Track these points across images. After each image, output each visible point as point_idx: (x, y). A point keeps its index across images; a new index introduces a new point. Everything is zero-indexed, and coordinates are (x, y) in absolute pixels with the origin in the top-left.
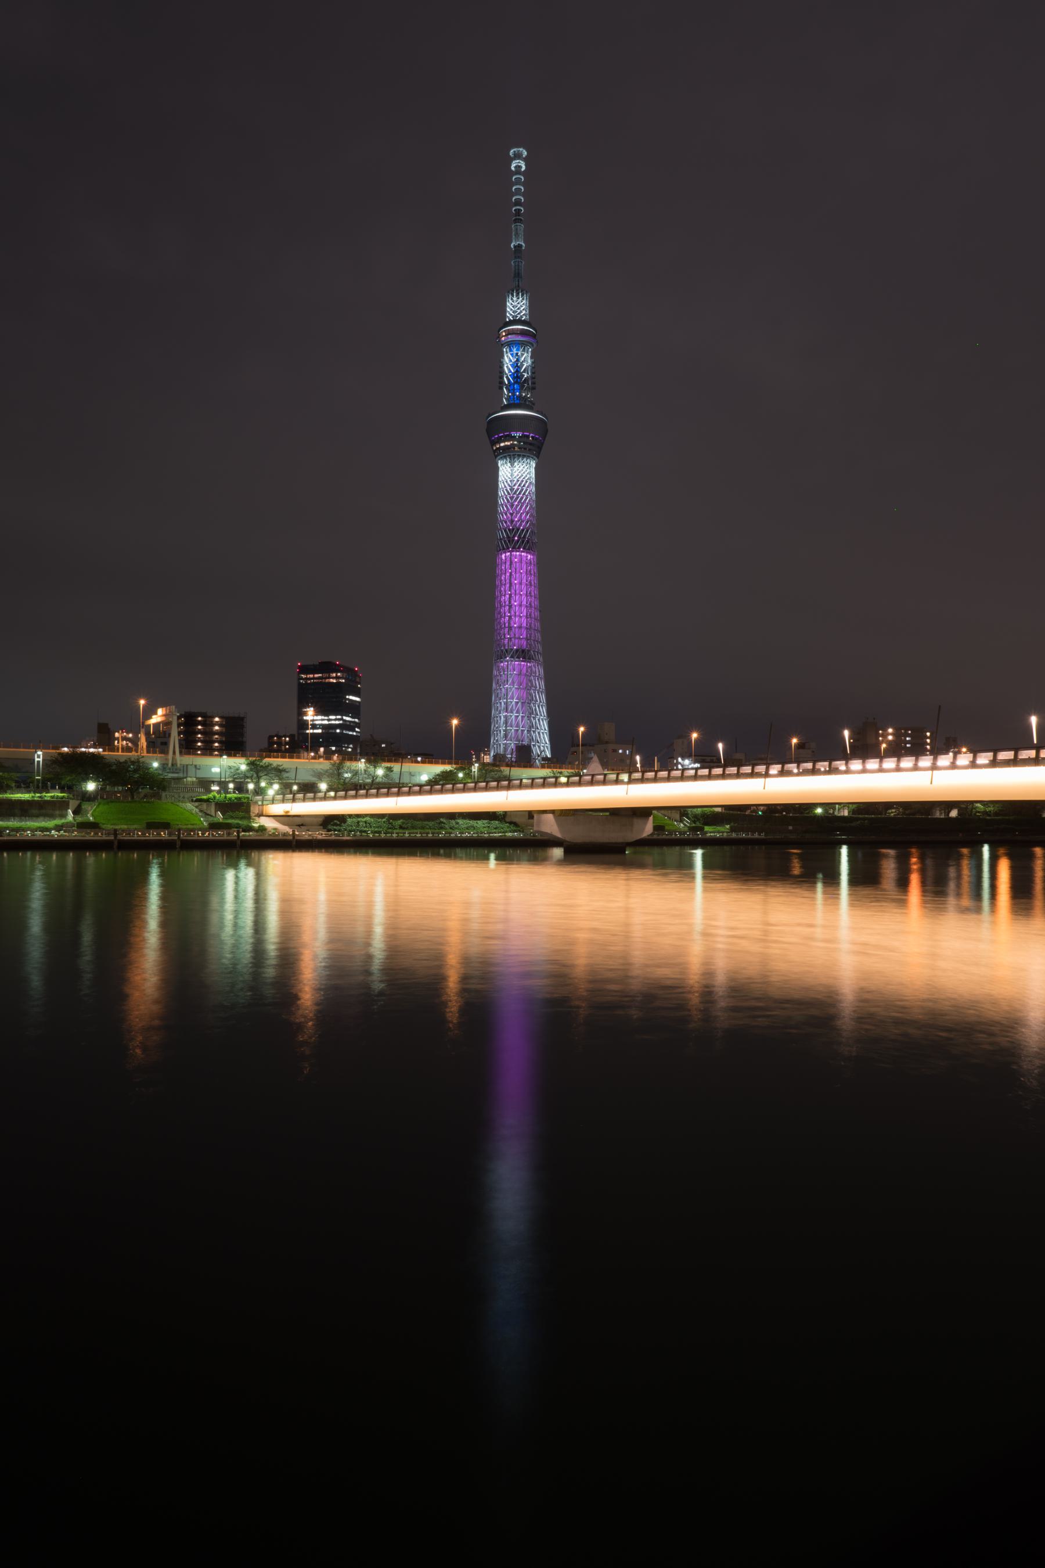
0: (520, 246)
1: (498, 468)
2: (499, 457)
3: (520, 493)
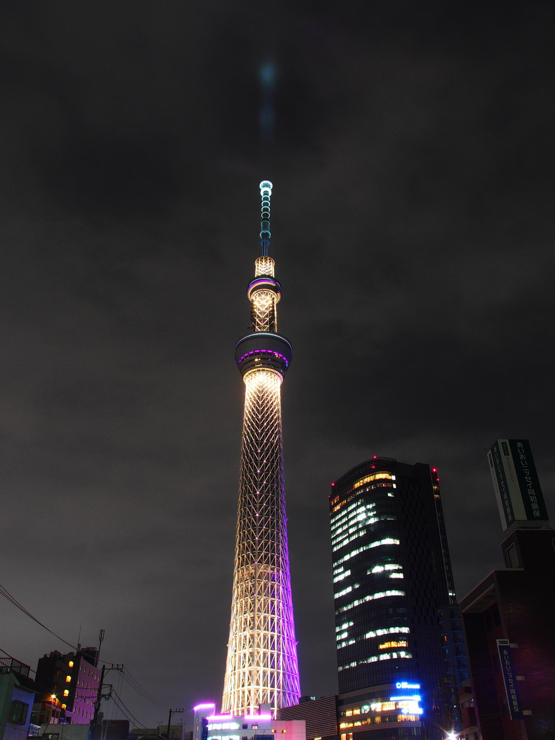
0: (267, 234)
1: (242, 387)
2: (247, 374)
3: (268, 403)
